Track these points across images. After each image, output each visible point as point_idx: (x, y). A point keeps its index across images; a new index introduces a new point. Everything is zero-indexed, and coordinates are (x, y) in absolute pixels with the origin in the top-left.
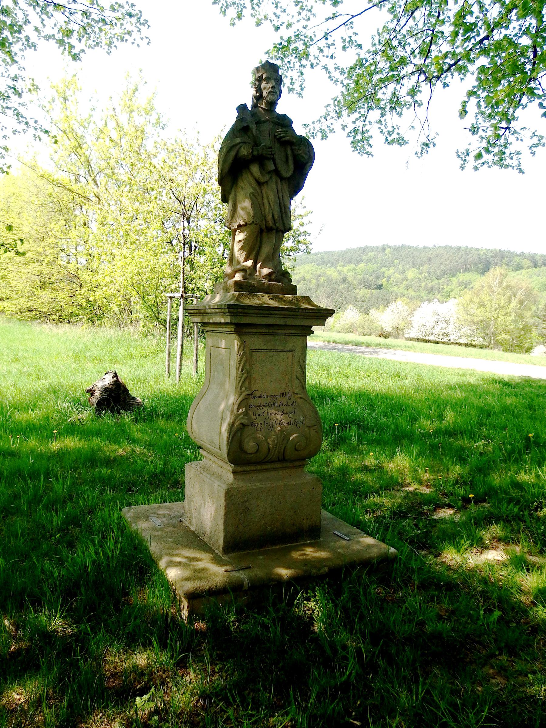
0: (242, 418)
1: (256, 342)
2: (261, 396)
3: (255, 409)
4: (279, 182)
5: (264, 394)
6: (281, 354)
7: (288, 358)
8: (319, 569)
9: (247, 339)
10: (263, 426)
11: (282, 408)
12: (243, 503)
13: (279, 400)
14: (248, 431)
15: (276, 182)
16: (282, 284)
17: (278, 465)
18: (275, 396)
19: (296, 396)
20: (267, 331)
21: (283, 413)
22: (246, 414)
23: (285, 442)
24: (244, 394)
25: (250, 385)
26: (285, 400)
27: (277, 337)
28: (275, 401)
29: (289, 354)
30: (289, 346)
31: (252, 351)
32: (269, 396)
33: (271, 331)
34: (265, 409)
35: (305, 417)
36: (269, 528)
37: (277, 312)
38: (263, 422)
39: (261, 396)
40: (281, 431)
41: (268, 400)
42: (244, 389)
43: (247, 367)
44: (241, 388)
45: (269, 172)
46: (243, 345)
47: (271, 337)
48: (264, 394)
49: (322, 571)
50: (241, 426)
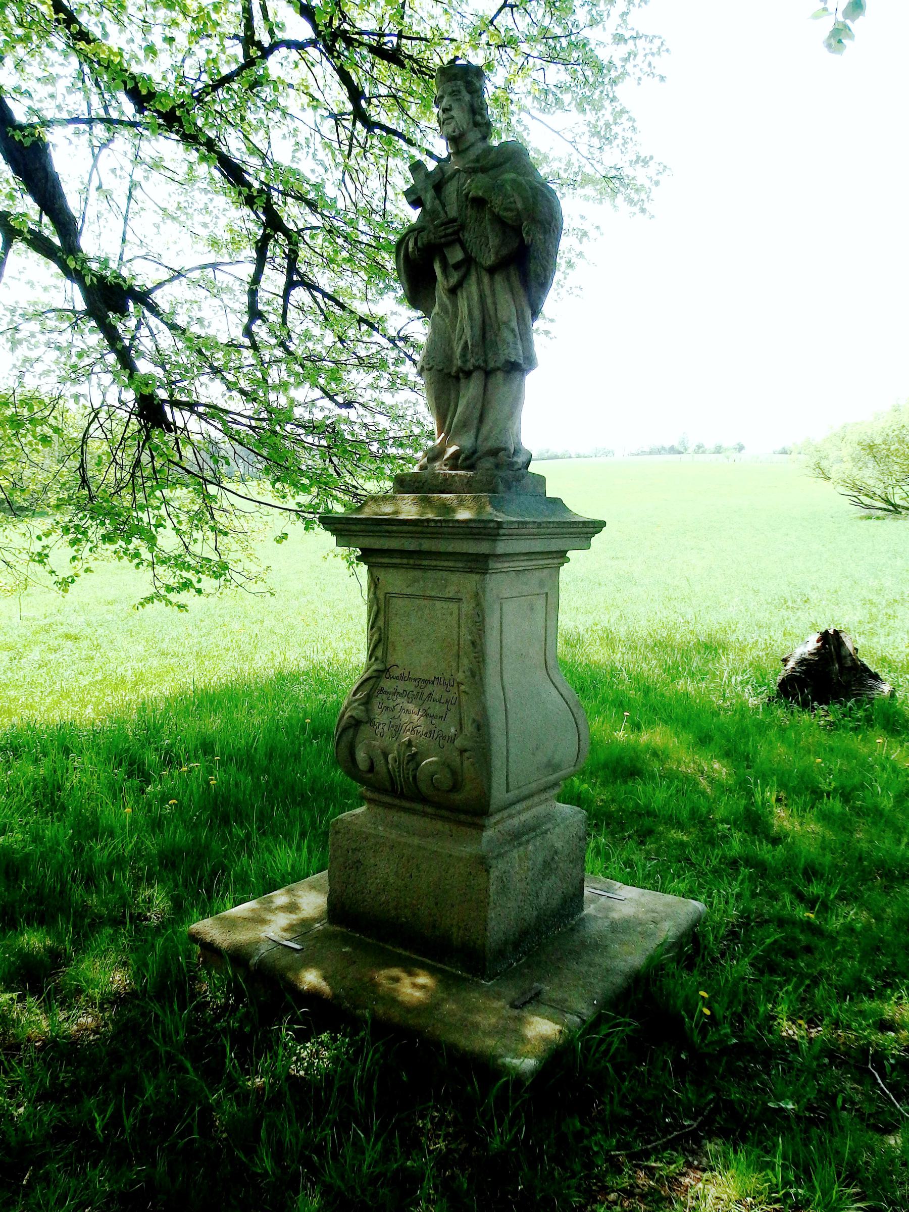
0: (355, 708)
1: (395, 581)
2: (402, 678)
3: (385, 696)
4: (486, 280)
5: (406, 675)
6: (438, 604)
7: (451, 614)
8: (356, 1008)
9: (381, 574)
10: (386, 729)
12: (354, 850)
13: (430, 688)
15: (479, 282)
16: (471, 473)
17: (419, 807)
18: (427, 681)
20: (405, 561)
23: (412, 766)
26: (437, 691)
27: (430, 574)
29: (453, 606)
30: (451, 591)
31: (388, 597)
32: (415, 679)
33: (411, 562)
34: (399, 700)
36: (393, 913)
37: (394, 528)
38: (387, 722)
40: (410, 744)
41: (410, 686)
43: (380, 623)
45: (457, 266)
46: (374, 583)
47: (418, 573)
48: (406, 675)
49: (359, 1012)
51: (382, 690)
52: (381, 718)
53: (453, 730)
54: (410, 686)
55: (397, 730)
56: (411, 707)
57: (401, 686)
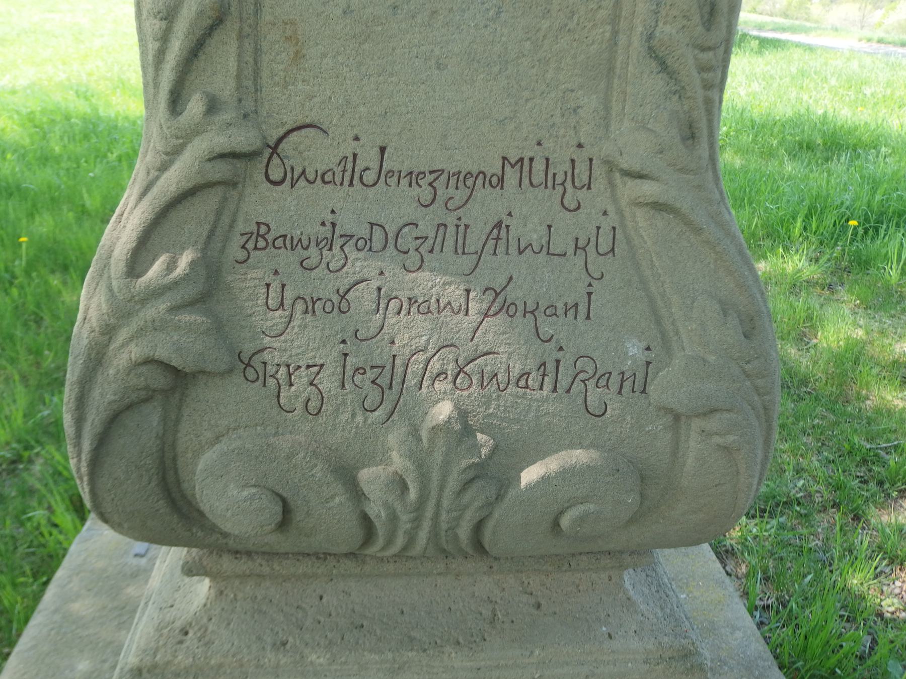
0: (158, 326)
2: (349, 172)
3: (286, 259)
10: (328, 382)
11: (494, 269)
13: (485, 207)
14: (221, 405)
18: (463, 178)
19: (630, 189)
21: (500, 302)
22: (207, 288)
23: (476, 497)
24: (199, 148)
25: (250, 78)
26: (529, 211)
28: (453, 209)
32: (414, 177)
34: (360, 264)
35: (662, 343)
38: (330, 357)
39: (349, 172)
40: (463, 428)
41: (398, 205)
42: (195, 107)
44: (176, 101)
50: (159, 380)
51: (260, 237)
52: (297, 342)
53: (634, 349)
54: (398, 205)
55: (387, 386)
56: (428, 282)
57: (353, 208)
